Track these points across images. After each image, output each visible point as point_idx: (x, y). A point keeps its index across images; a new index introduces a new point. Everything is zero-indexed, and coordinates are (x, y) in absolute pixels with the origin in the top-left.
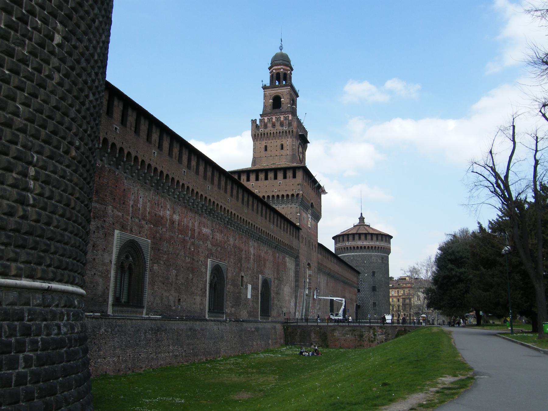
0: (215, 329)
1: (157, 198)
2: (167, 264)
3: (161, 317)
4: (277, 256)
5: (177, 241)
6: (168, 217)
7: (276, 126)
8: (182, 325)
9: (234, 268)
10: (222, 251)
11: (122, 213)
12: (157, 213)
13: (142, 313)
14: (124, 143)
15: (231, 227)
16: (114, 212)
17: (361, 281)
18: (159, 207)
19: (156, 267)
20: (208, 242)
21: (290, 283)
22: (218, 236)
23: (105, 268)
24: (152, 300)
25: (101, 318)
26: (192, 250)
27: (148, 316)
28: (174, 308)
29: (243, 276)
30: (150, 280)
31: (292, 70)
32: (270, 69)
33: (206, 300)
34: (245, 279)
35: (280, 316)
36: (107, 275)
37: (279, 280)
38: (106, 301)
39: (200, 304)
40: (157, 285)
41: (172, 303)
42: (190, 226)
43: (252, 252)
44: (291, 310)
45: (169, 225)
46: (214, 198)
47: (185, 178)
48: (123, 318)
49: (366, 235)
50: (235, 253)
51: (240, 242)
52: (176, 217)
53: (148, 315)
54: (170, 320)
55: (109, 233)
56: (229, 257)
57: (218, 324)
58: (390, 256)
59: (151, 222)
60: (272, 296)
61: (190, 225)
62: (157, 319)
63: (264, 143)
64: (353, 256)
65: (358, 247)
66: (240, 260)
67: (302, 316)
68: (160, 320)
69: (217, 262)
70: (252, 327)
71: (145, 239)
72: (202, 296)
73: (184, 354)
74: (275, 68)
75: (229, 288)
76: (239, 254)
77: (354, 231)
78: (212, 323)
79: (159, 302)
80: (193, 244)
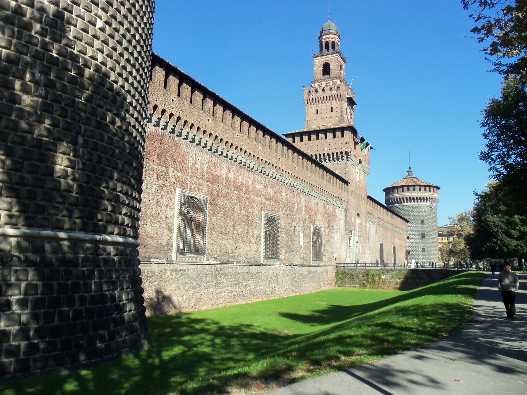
0: (270, 273)
1: (213, 160)
6: (224, 176)
7: (325, 91)
11: (182, 174)
14: (181, 113)
16: (175, 173)
19: (214, 219)
20: (262, 197)
22: (271, 191)
23: (168, 221)
25: (167, 264)
27: (208, 262)
28: (232, 255)
30: (210, 230)
34: (297, 228)
35: (331, 260)
36: (170, 227)
37: (330, 229)
38: (170, 249)
41: (230, 251)
47: (238, 141)
52: (231, 176)
53: (209, 261)
59: (209, 181)
60: (323, 243)
61: (245, 182)
70: (305, 270)
71: (204, 196)
73: (242, 294)
75: (282, 236)
76: (291, 206)
79: (218, 249)
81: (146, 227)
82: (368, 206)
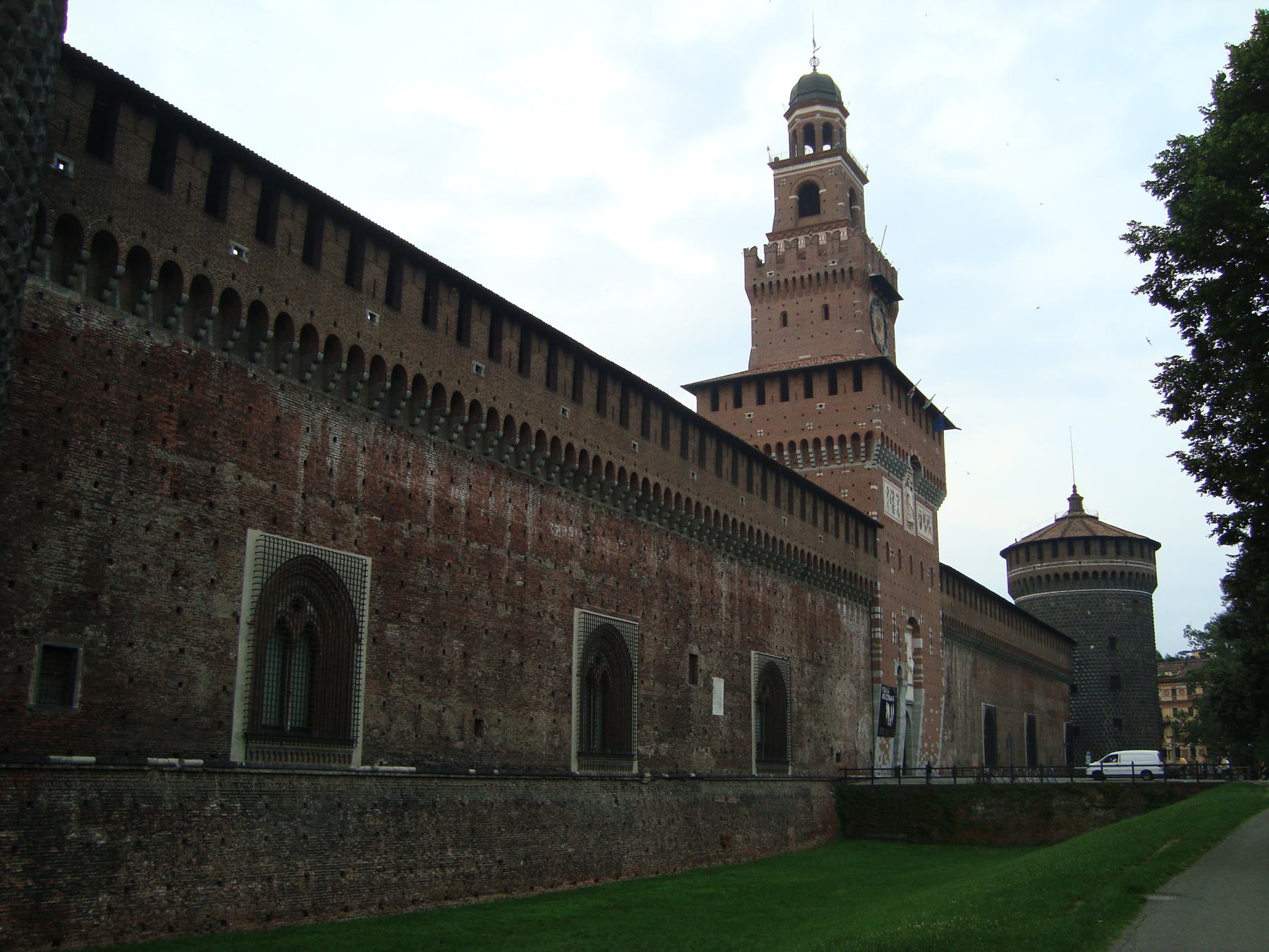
0: (604, 802)
1: (391, 441)
2: (432, 624)
3: (414, 769)
5: (465, 559)
6: (433, 495)
8: (491, 793)
9: (665, 633)
10: (621, 587)
11: (272, 483)
12: (392, 481)
13: (348, 758)
14: (266, 290)
15: (650, 520)
16: (244, 479)
17: (1079, 663)
18: (398, 467)
19: (392, 631)
20: (575, 564)
21: (854, 673)
22: (607, 546)
23: (216, 633)
24: (383, 721)
25: (208, 773)
26: (519, 583)
27: (368, 768)
28: (459, 745)
29: (696, 656)
30: (375, 667)
31: (846, 113)
32: (787, 115)
33: (570, 722)
34: (702, 664)
35: (823, 761)
36: (226, 653)
38: (224, 725)
39: (552, 734)
40: (399, 682)
41: (453, 732)
42: (509, 518)
43: (724, 588)
44: (860, 747)
45: (436, 516)
46: (585, 441)
47: (481, 386)
48: (282, 771)
49: (1087, 541)
50: (666, 591)
51: (683, 561)
52: (459, 494)
53: (372, 765)
54: (448, 778)
55: (228, 537)
56: (645, 603)
57: (615, 788)
58: (1156, 596)
60: (795, 709)
61: (509, 515)
62: (398, 775)
63: (777, 307)
64: (1056, 597)
65: (1066, 575)
66: (684, 611)
67: (895, 760)
68: (410, 777)
69: (604, 616)
70: (730, 792)
71: (353, 555)
72: (556, 711)
73: (495, 870)
74: (798, 112)
75: (645, 689)
76: (680, 594)
77: (1056, 534)
78: (595, 783)
79: (409, 727)
80: (520, 567)
81: (129, 650)
82: (945, 596)
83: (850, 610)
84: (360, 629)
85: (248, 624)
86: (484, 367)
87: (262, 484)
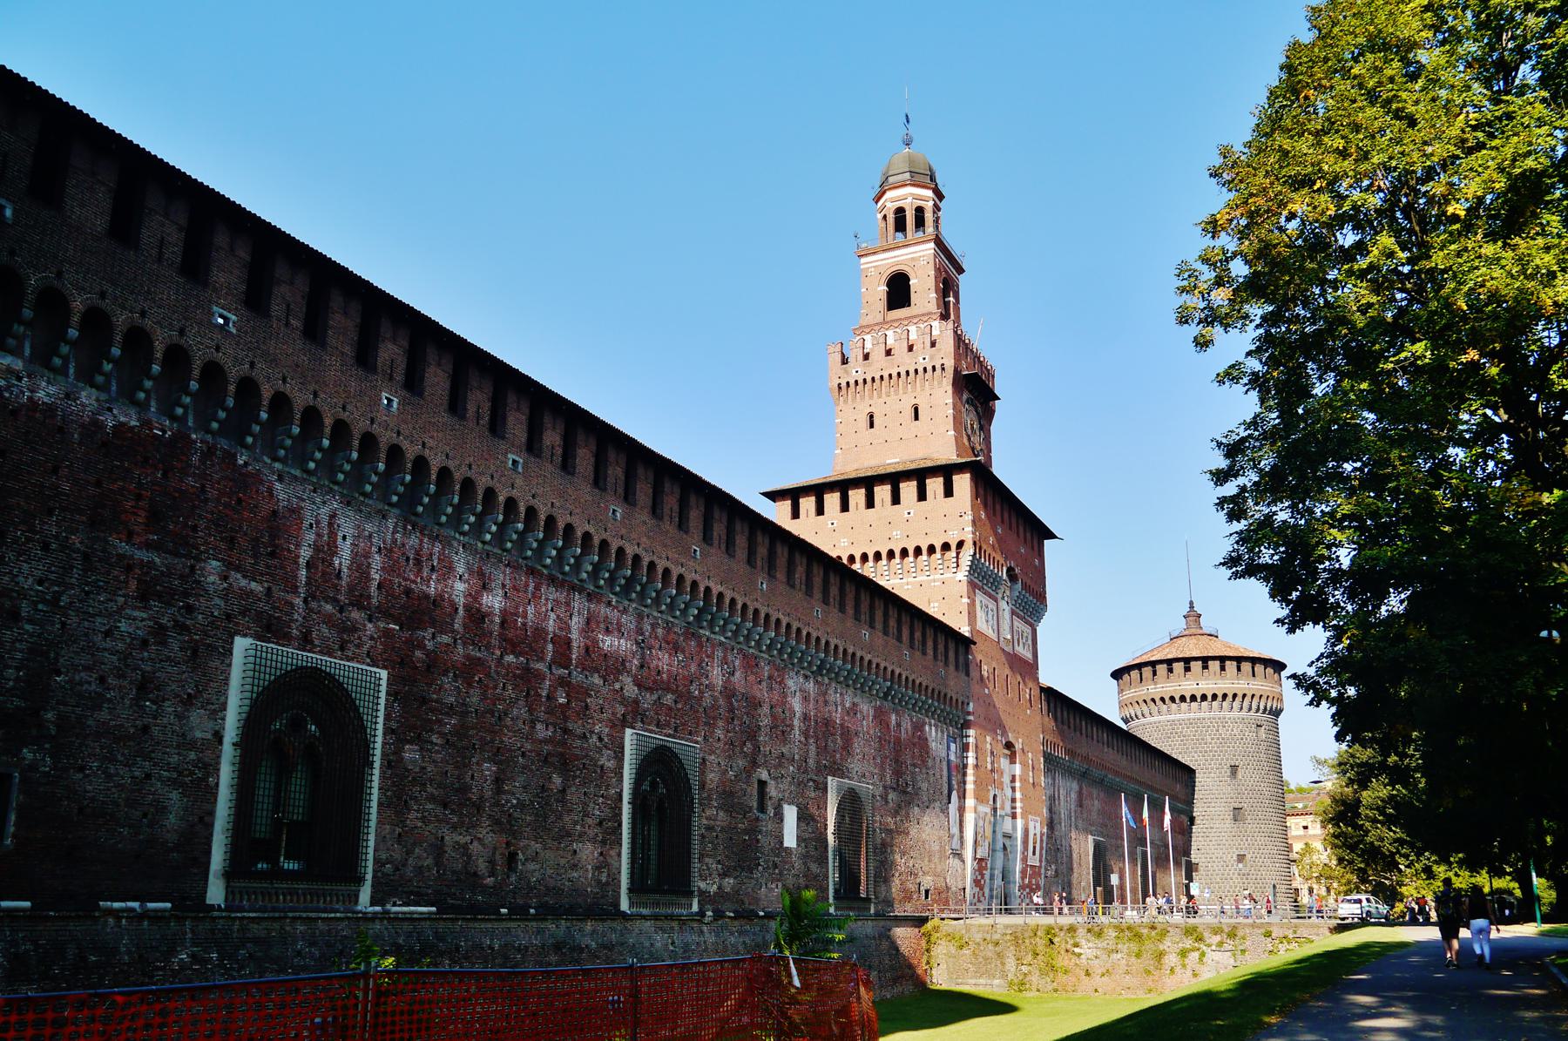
1: (413, 541)
2: (460, 745)
3: (434, 909)
4: (894, 722)
5: (498, 673)
6: (461, 601)
9: (730, 757)
10: (680, 706)
11: (266, 585)
12: (413, 586)
18: (420, 570)
19: (411, 754)
22: (663, 661)
23: (192, 755)
26: (562, 700)
27: (378, 909)
28: (489, 881)
29: (765, 782)
33: (619, 855)
34: (772, 791)
36: (205, 779)
37: (905, 792)
39: (598, 868)
40: (418, 811)
41: (482, 866)
42: (551, 629)
45: (465, 626)
46: (638, 544)
47: (519, 482)
48: (271, 915)
50: (731, 710)
51: (751, 678)
52: (493, 601)
53: (383, 905)
54: (476, 920)
55: (209, 645)
57: (672, 928)
59: (391, 616)
61: (551, 625)
62: (415, 916)
66: (752, 734)
68: (429, 919)
69: (660, 737)
72: (604, 842)
75: (707, 817)
78: (649, 923)
79: (429, 862)
80: (563, 682)
81: (80, 776)
82: (1047, 719)
83: (939, 734)
84: (371, 752)
85: (234, 744)
86: (521, 461)
87: (253, 585)
